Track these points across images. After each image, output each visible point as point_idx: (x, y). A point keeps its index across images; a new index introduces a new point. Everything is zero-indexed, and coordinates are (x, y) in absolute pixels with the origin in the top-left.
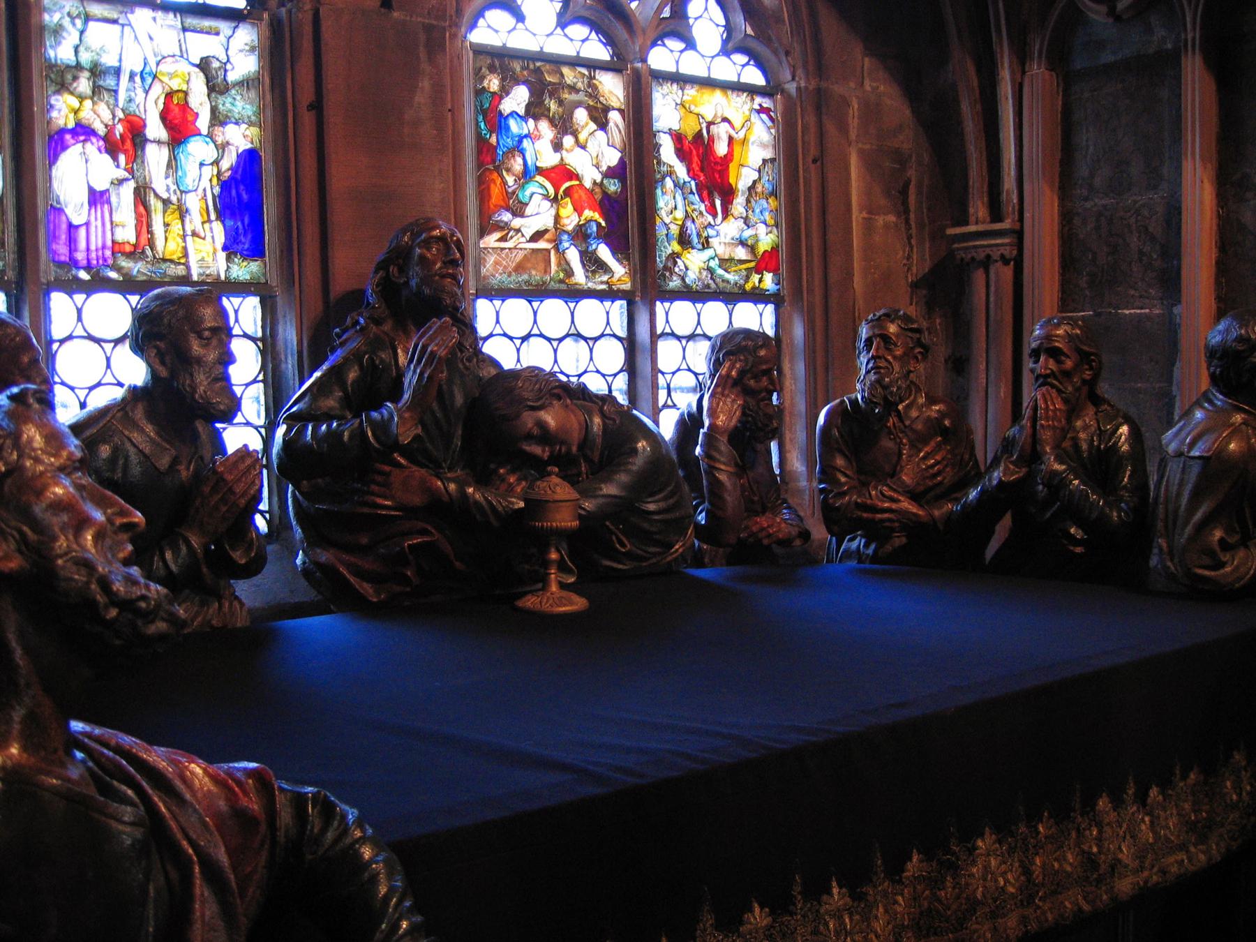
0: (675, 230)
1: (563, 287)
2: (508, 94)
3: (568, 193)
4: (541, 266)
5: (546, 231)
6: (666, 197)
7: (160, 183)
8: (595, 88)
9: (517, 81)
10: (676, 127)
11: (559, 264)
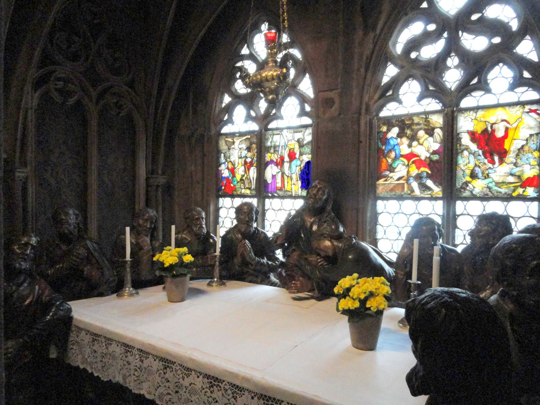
0: (468, 172)
1: (410, 196)
2: (390, 131)
3: (413, 162)
4: (401, 189)
5: (403, 177)
6: (464, 159)
7: (287, 172)
8: (429, 121)
9: (394, 126)
10: (471, 129)
11: (408, 188)
